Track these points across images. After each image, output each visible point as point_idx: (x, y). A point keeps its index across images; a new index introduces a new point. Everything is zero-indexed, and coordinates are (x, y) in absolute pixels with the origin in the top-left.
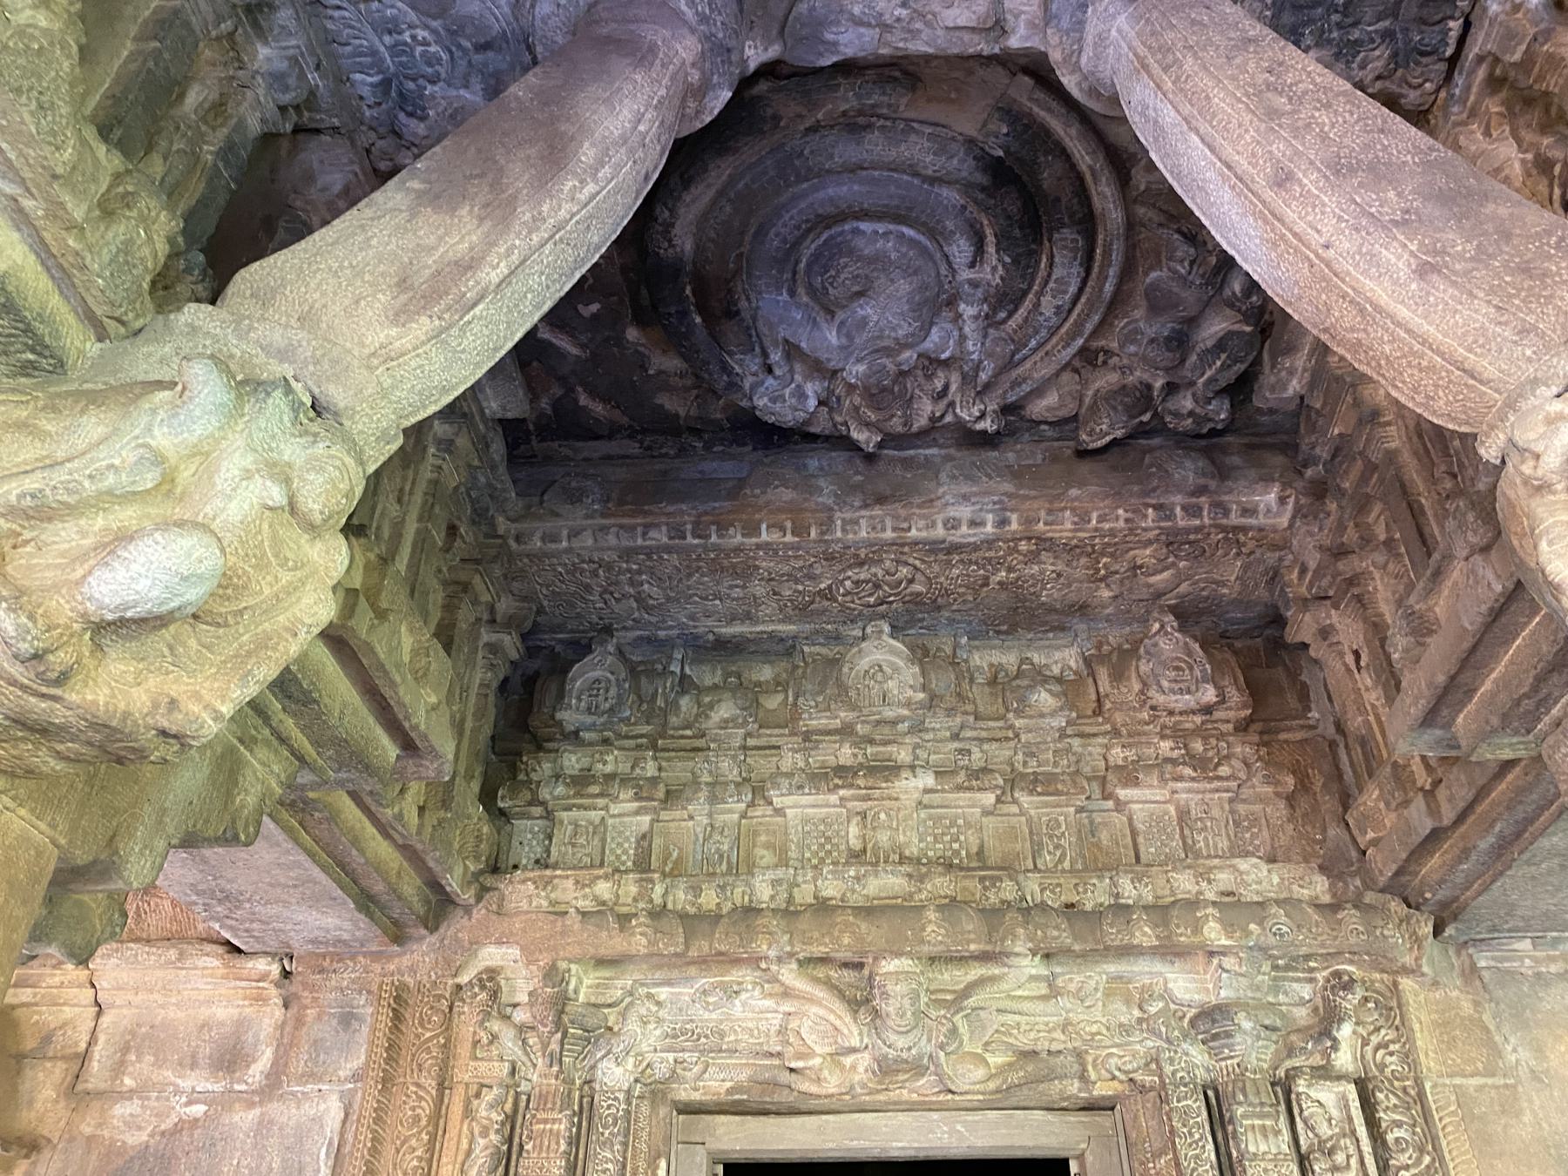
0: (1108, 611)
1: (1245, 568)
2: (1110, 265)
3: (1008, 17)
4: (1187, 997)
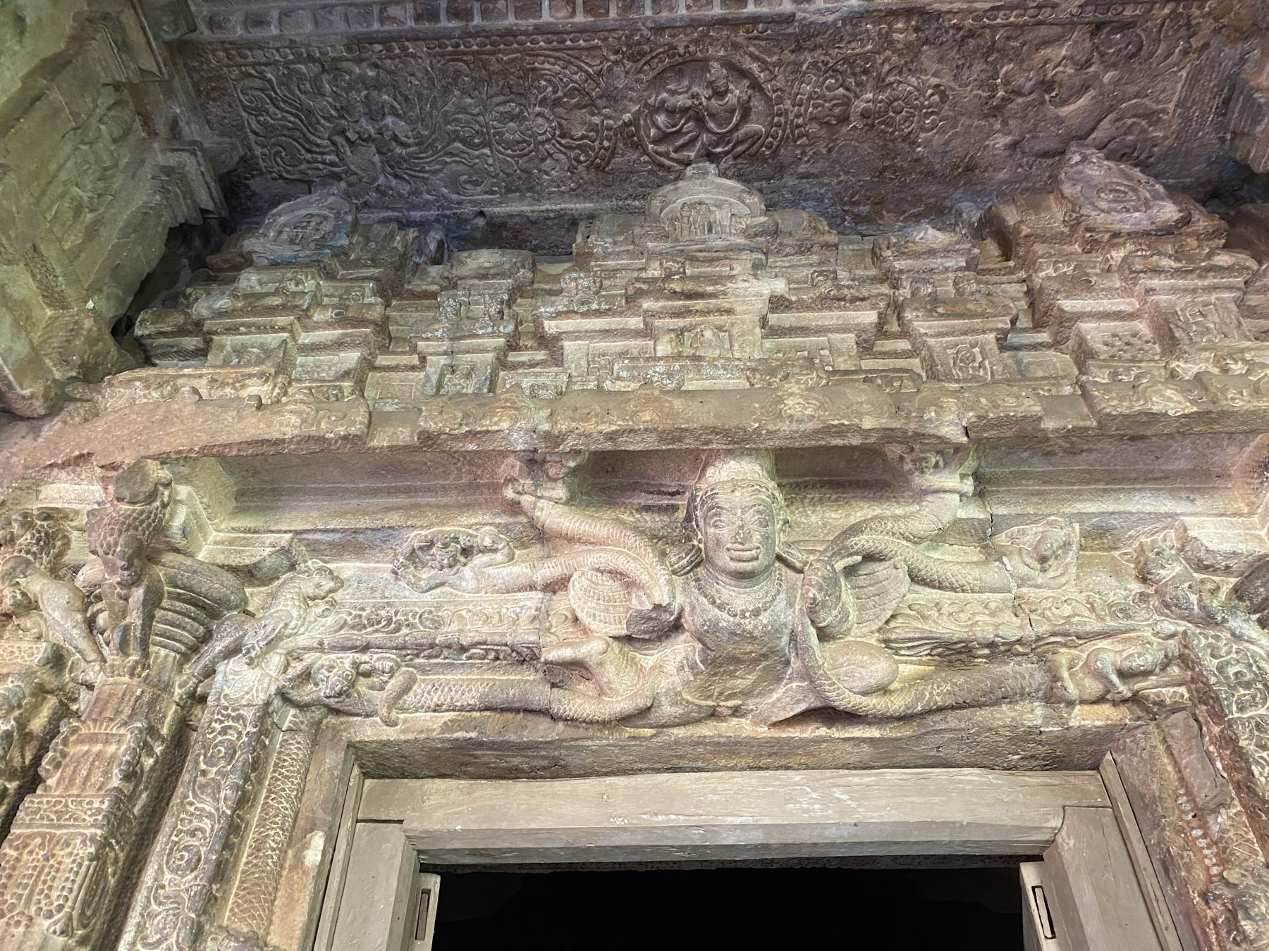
0: (1002, 175)
1: (1193, 81)
4: (1227, 547)
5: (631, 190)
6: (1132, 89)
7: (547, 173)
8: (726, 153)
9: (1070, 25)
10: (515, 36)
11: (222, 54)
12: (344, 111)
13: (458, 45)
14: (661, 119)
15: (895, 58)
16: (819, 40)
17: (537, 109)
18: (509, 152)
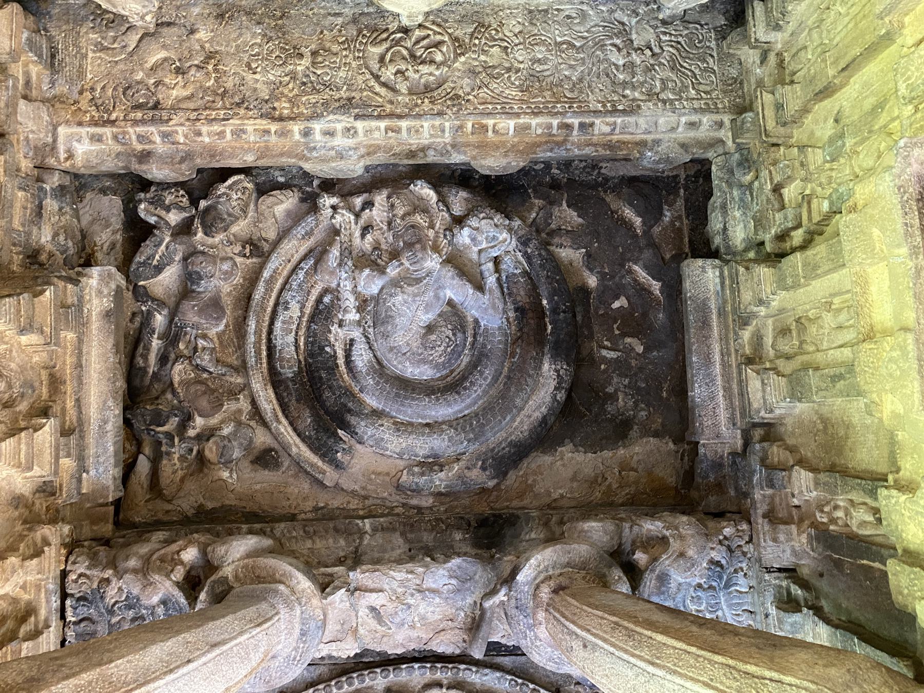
0: (196, 10)
1: (81, 73)
2: (255, 343)
3: (346, 599)
5: (460, 8)
6: (121, 66)
7: (519, 23)
8: (393, 33)
9: (175, 109)
10: (533, 112)
11: (720, 106)
12: (649, 69)
13: (570, 108)
14: (439, 58)
15: (286, 91)
16: (337, 104)
17: (522, 66)
18: (543, 38)
